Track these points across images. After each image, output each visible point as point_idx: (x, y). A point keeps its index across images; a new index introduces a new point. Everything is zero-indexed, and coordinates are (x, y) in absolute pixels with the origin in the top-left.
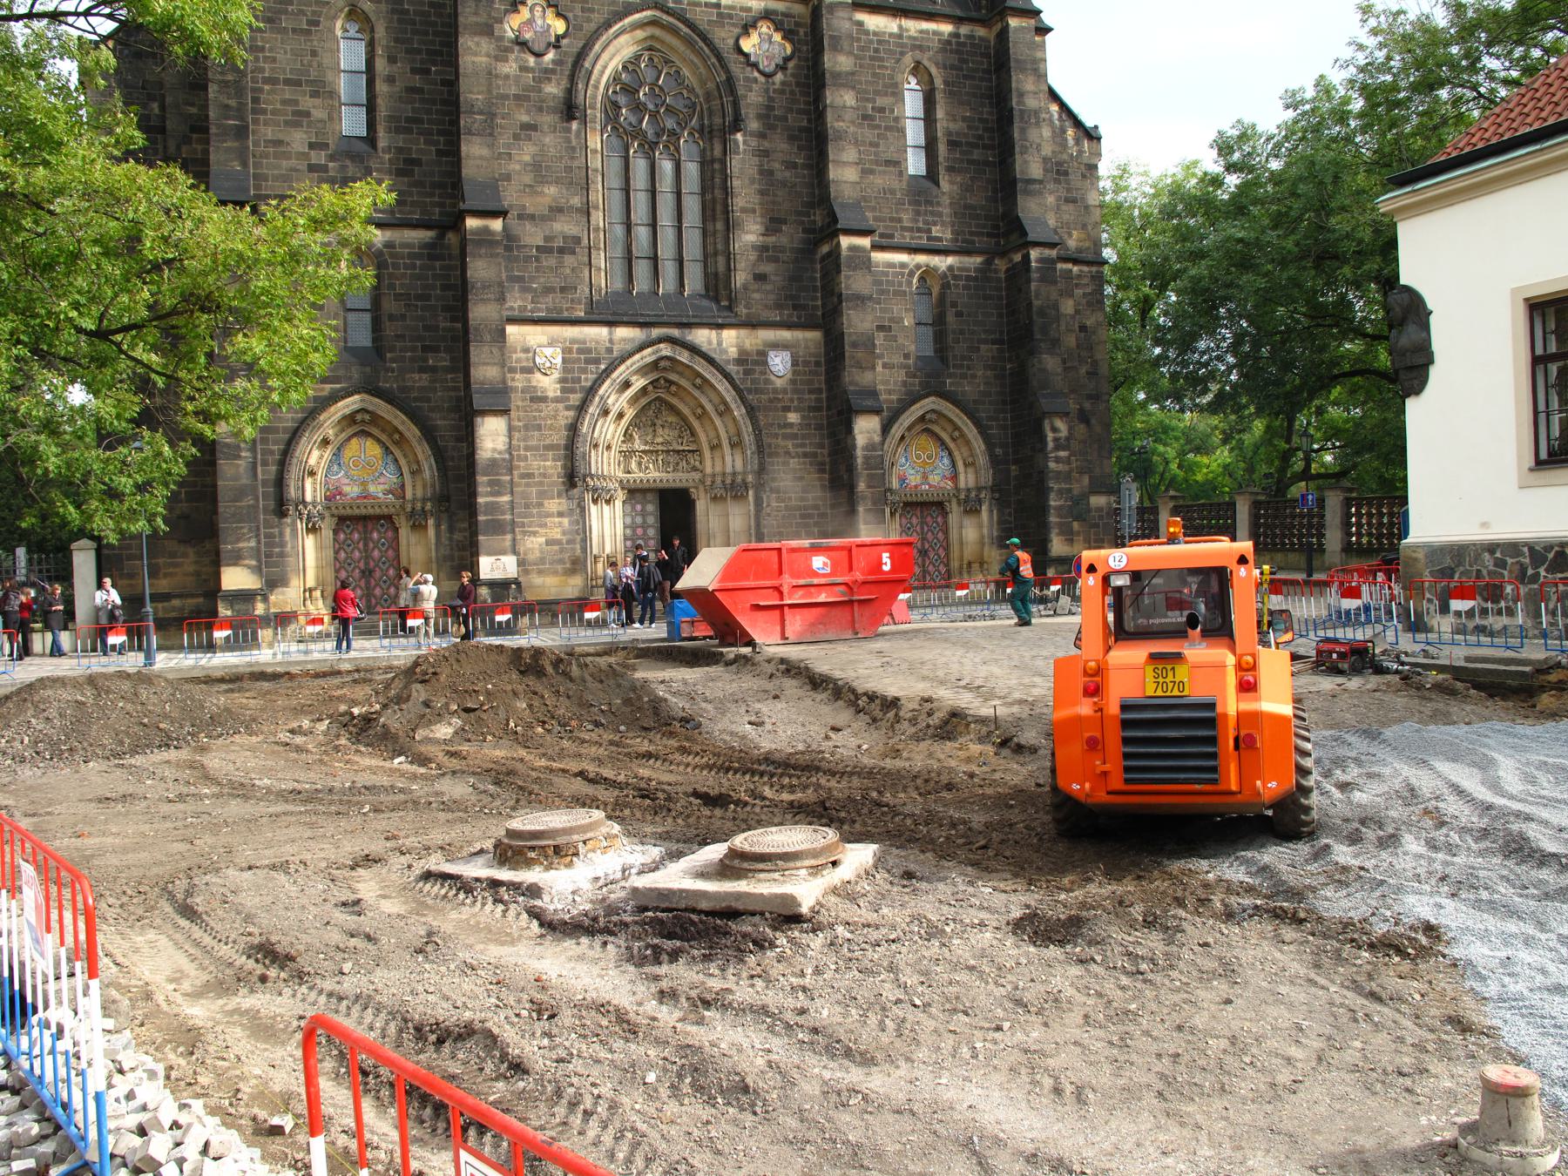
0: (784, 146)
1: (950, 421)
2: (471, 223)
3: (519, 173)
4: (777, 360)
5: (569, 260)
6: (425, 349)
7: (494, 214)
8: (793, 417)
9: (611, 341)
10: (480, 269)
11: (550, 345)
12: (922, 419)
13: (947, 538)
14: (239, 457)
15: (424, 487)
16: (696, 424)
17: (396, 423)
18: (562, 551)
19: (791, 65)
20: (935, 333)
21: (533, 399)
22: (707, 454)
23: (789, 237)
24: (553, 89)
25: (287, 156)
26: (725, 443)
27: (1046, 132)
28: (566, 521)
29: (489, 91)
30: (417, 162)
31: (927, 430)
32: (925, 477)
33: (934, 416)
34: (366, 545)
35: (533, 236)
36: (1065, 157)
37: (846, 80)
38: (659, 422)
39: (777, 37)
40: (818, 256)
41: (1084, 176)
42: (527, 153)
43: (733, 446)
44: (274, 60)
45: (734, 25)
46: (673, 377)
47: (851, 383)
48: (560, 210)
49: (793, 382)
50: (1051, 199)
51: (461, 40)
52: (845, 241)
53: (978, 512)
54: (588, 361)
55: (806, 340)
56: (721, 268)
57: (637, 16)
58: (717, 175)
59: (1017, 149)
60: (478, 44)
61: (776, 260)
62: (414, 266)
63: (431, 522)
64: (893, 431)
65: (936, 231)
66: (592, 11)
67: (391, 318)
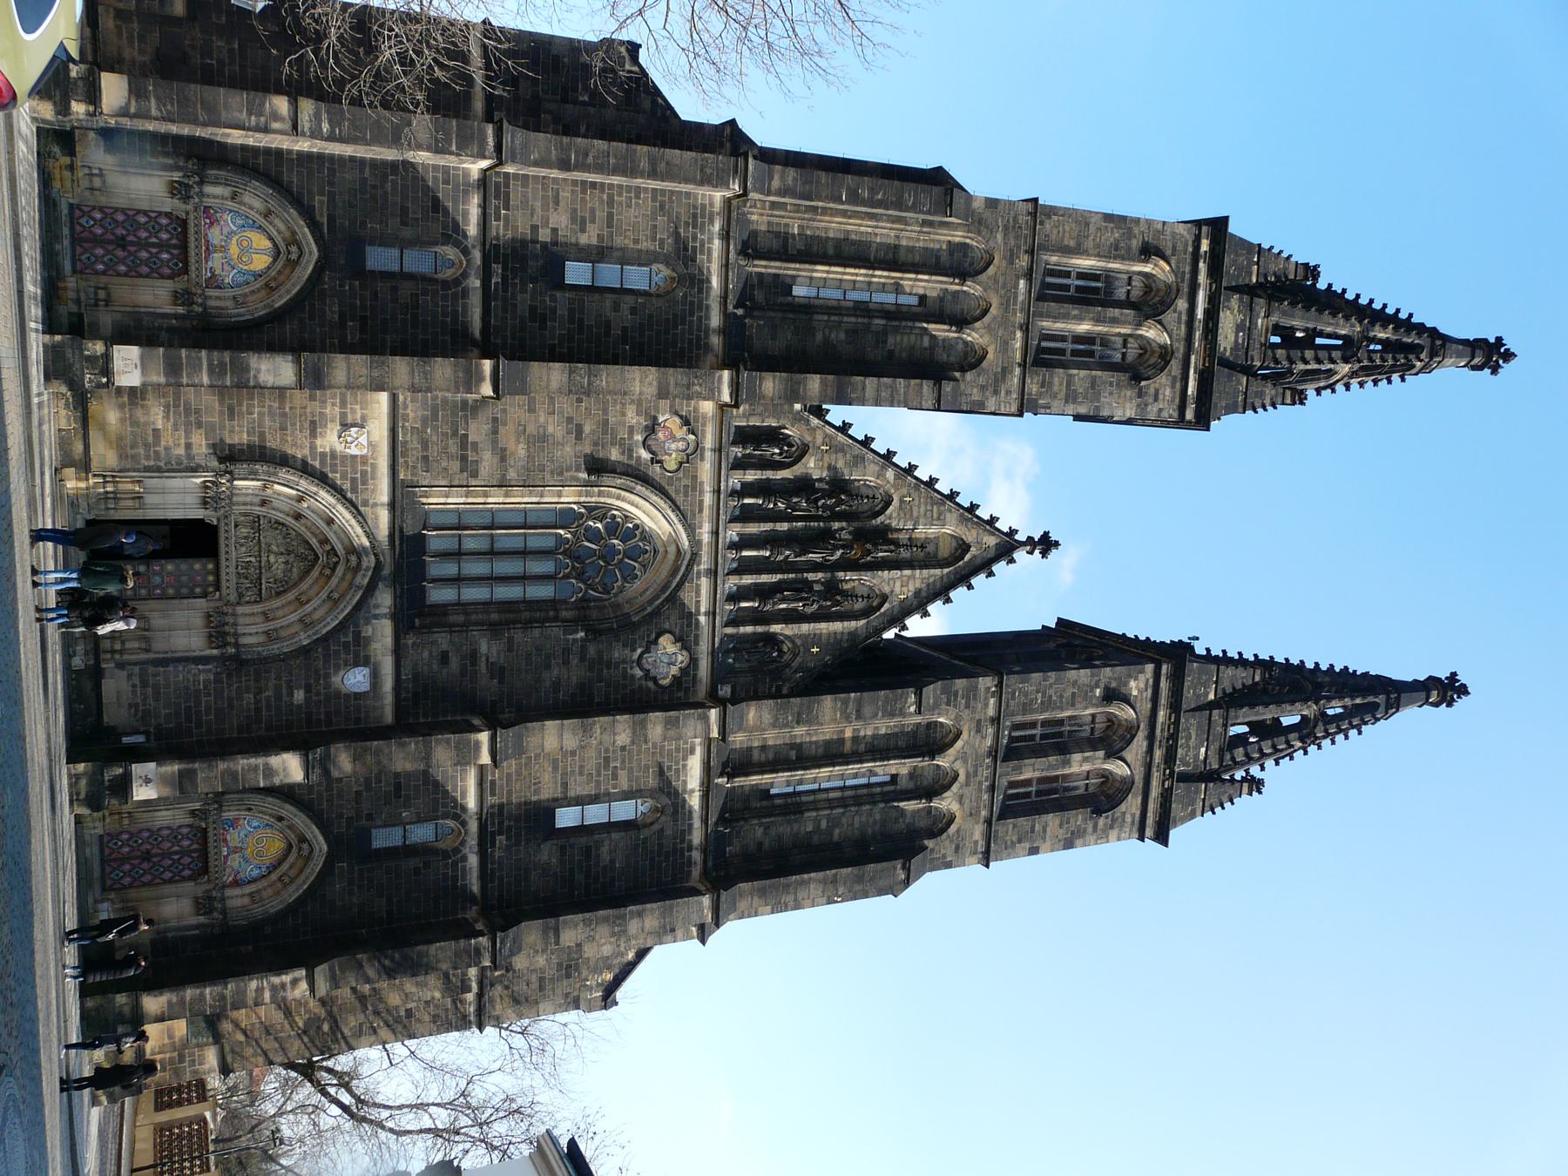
0: (574, 680)
1: (301, 871)
2: (487, 365)
3: (536, 421)
4: (360, 678)
5: (455, 466)
6: (363, 319)
7: (496, 389)
8: (299, 696)
9: (375, 505)
10: (443, 369)
11: (370, 444)
12: (302, 839)
13: (165, 882)
14: (250, 113)
15: (217, 308)
16: (291, 596)
17: (289, 285)
18: (146, 445)
19: (651, 684)
20: (396, 848)
21: (313, 423)
22: (258, 608)
23: (486, 685)
24: (614, 455)
25: (545, 207)
26: (271, 625)
27: (607, 950)
28: (181, 451)
29: (609, 392)
30: (543, 327)
31: (290, 846)
32: (236, 850)
33: (305, 853)
34: (153, 245)
35: (477, 431)
36: (585, 973)
37: (639, 734)
38: (291, 558)
39: (674, 670)
40: (468, 717)
41: (567, 995)
42: (555, 429)
43: (266, 633)
44: (629, 206)
45: (682, 627)
46: (340, 570)
47: (337, 749)
48: (503, 459)
49: (338, 694)
50: (541, 961)
51: (653, 369)
52: (484, 737)
53: (198, 915)
54: (354, 480)
55: (382, 707)
56: (452, 619)
57: (684, 536)
58: (543, 614)
59: (587, 915)
60: (650, 384)
61: (463, 673)
62: (445, 315)
63: (180, 310)
64: (288, 806)
65: (501, 840)
66: (686, 495)
67: (394, 289)
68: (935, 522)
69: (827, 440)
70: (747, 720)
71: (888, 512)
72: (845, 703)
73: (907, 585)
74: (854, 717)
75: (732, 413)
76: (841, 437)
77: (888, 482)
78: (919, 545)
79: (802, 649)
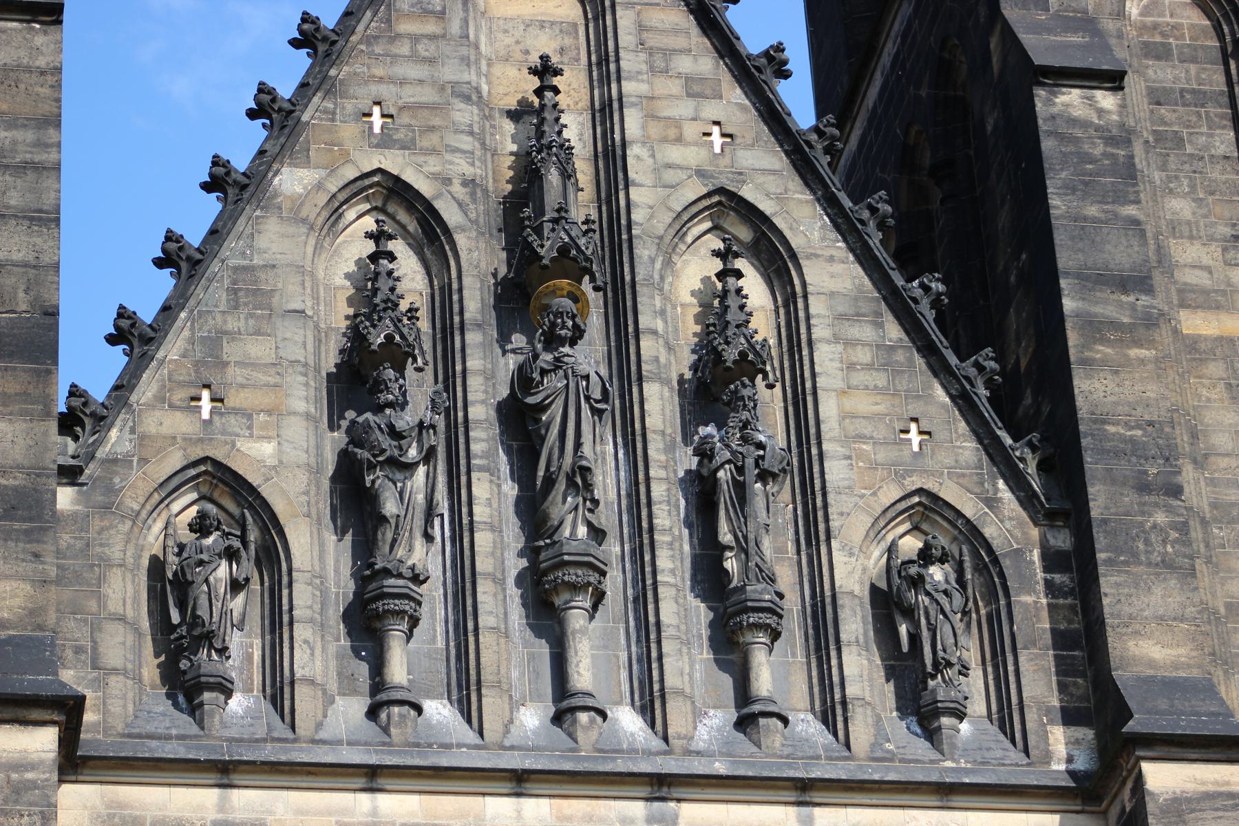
68: (455, 28)
69: (180, 395)
70: (1176, 666)
71: (424, 187)
72: (1096, 328)
73: (677, 123)
74: (1145, 300)
75: (95, 727)
76: (173, 349)
77: (319, 186)
78: (535, 82)
79: (914, 483)
